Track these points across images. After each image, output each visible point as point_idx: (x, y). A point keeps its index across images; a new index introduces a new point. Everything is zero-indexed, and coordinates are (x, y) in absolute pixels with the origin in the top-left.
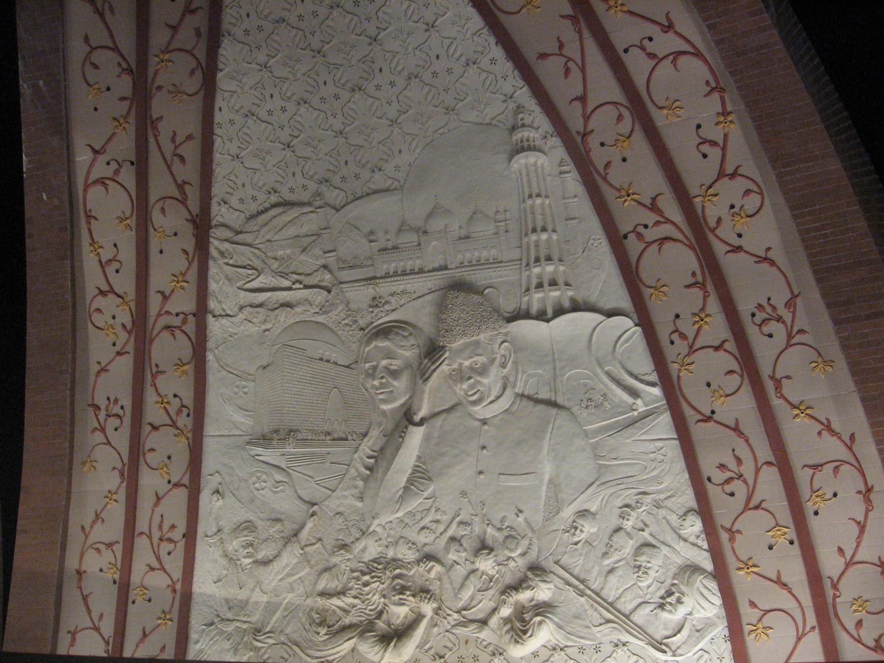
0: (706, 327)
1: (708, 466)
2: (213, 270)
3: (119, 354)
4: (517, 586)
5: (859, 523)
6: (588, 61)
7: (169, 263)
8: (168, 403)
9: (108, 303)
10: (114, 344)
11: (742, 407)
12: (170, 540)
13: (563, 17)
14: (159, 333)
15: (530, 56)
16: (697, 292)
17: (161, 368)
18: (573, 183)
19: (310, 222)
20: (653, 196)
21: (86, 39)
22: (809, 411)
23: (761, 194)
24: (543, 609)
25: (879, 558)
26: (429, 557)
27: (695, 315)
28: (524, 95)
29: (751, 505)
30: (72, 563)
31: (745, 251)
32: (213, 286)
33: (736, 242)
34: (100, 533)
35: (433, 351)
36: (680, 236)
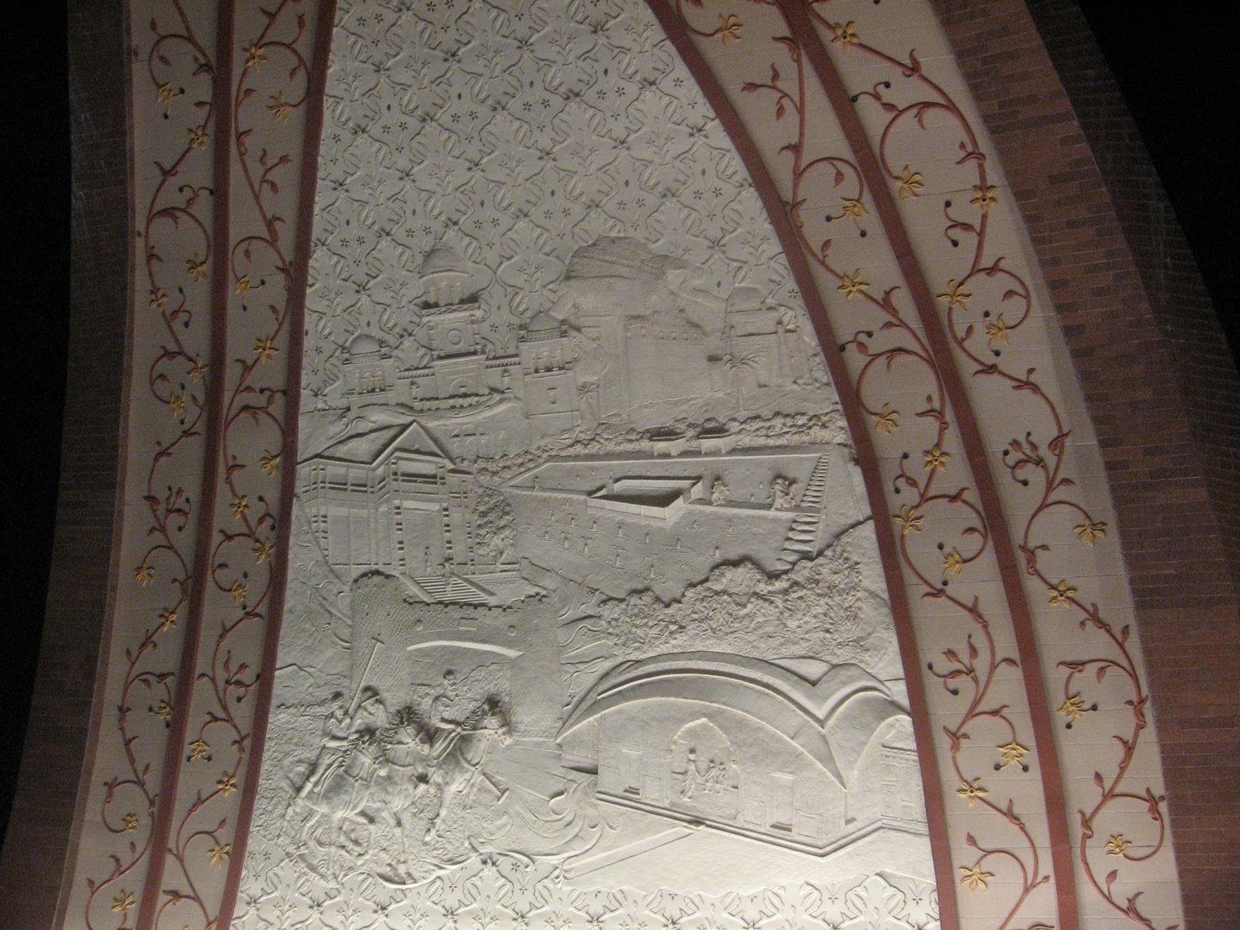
0: (941, 469)
3: (187, 433)
5: (1125, 743)
6: (807, 99)
8: (246, 506)
10: (182, 422)
12: (239, 683)
13: (776, 39)
14: (237, 415)
15: (733, 89)
16: (931, 424)
17: (239, 462)
20: (887, 289)
21: (153, 26)
22: (1069, 594)
23: (1027, 297)
25: (1148, 790)
27: (927, 452)
31: (1000, 373)
33: (990, 359)
36: (916, 347)
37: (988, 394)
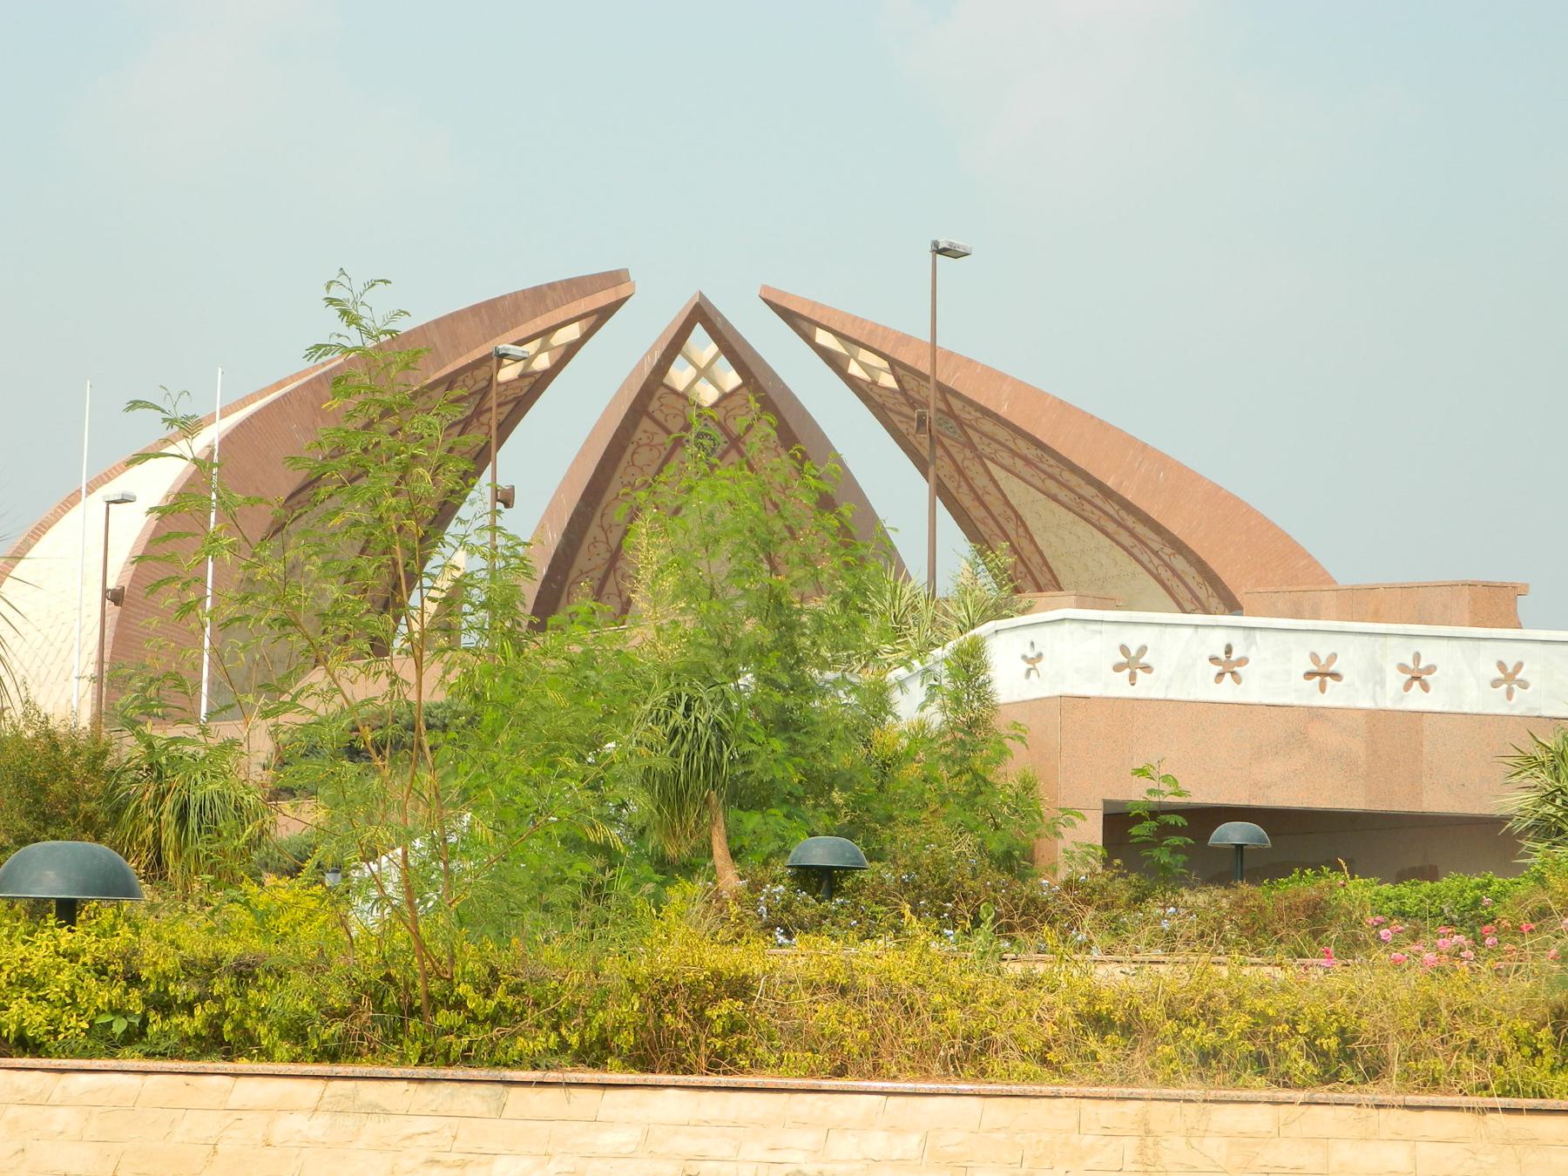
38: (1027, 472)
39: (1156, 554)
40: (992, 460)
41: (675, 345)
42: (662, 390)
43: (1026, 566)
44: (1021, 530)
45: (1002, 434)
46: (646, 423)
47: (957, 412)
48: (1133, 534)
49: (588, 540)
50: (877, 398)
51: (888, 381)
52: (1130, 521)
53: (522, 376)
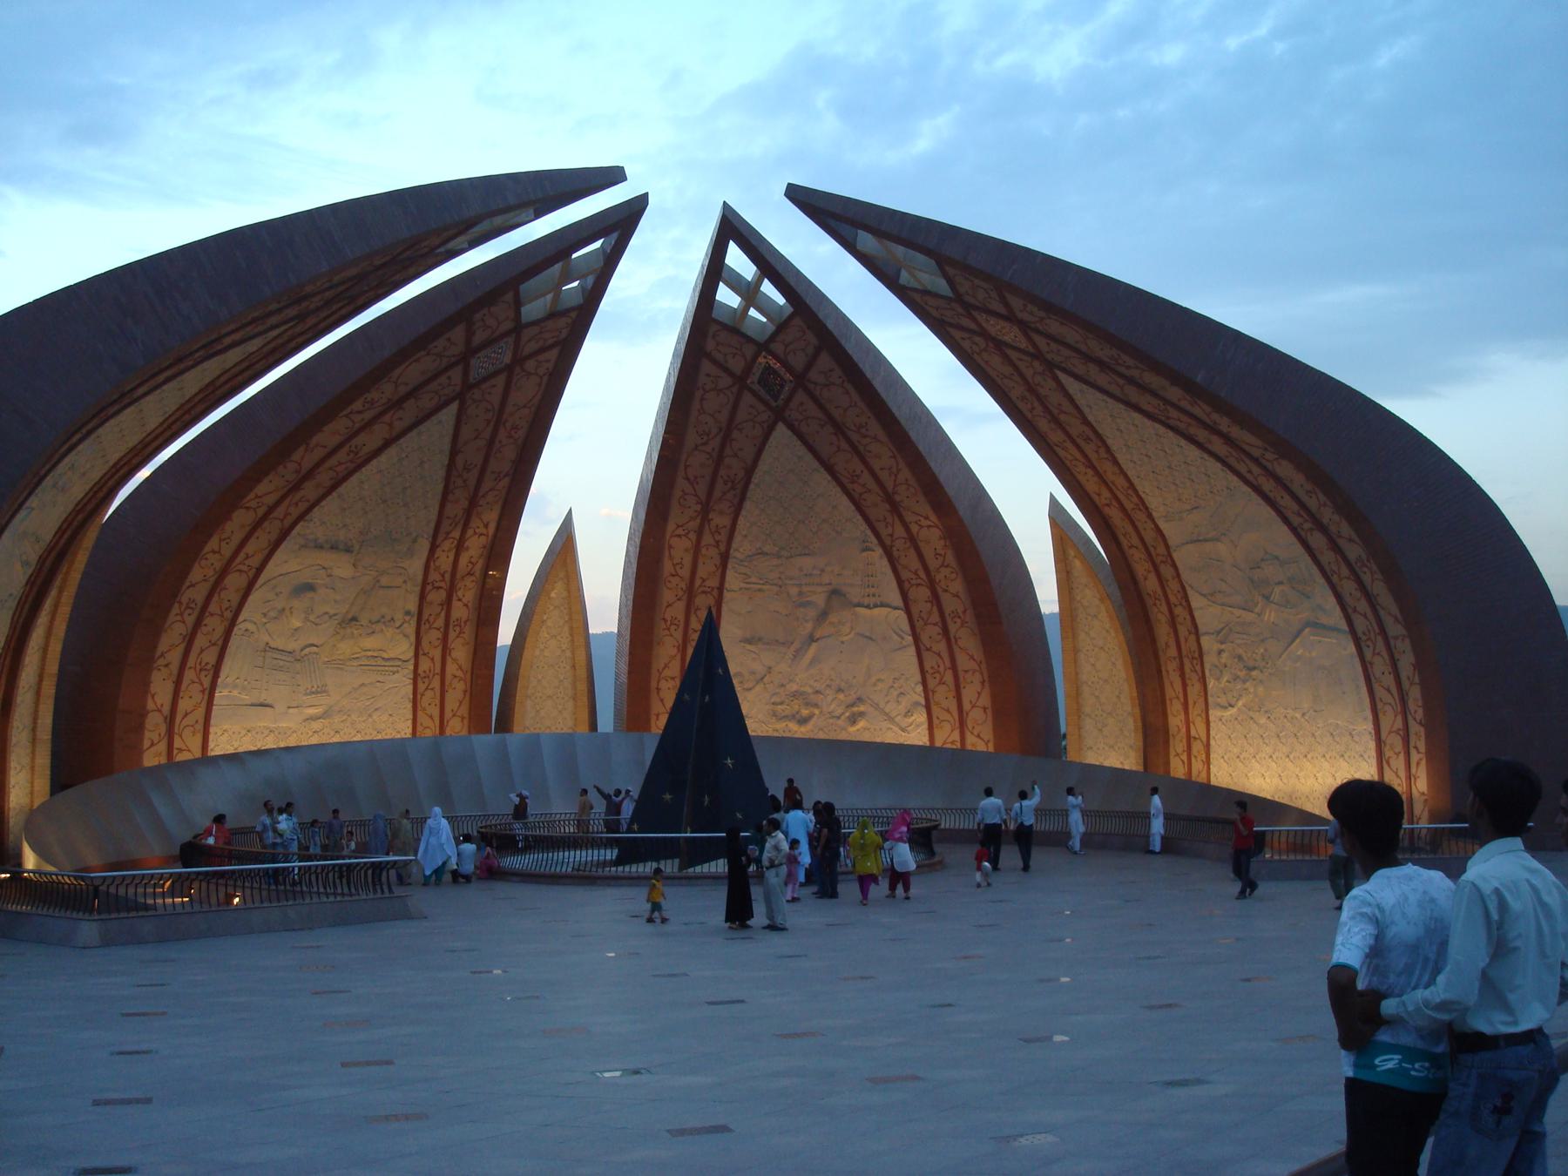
1: (927, 667)
2: (730, 574)
4: (852, 705)
7: (706, 568)
9: (675, 580)
11: (941, 647)
18: (885, 562)
19: (775, 562)
24: (862, 714)
26: (817, 692)
28: (869, 532)
29: (942, 683)
30: (653, 684)
32: (728, 578)
34: (667, 673)
35: (823, 615)
37: (946, 599)
38: (1103, 380)
39: (1256, 461)
40: (1065, 370)
41: (715, 271)
42: (714, 328)
43: (1110, 490)
44: (1102, 450)
45: (1071, 335)
46: (707, 366)
47: (1020, 315)
48: (1228, 440)
49: (677, 493)
50: (934, 313)
51: (942, 286)
52: (1224, 424)
53: (553, 315)
